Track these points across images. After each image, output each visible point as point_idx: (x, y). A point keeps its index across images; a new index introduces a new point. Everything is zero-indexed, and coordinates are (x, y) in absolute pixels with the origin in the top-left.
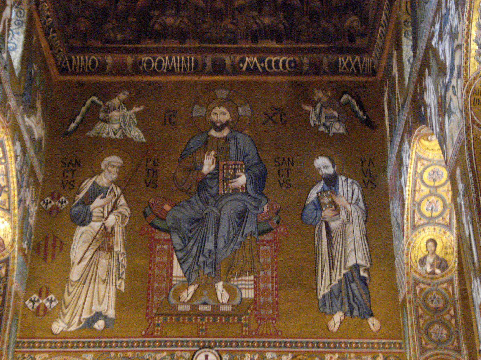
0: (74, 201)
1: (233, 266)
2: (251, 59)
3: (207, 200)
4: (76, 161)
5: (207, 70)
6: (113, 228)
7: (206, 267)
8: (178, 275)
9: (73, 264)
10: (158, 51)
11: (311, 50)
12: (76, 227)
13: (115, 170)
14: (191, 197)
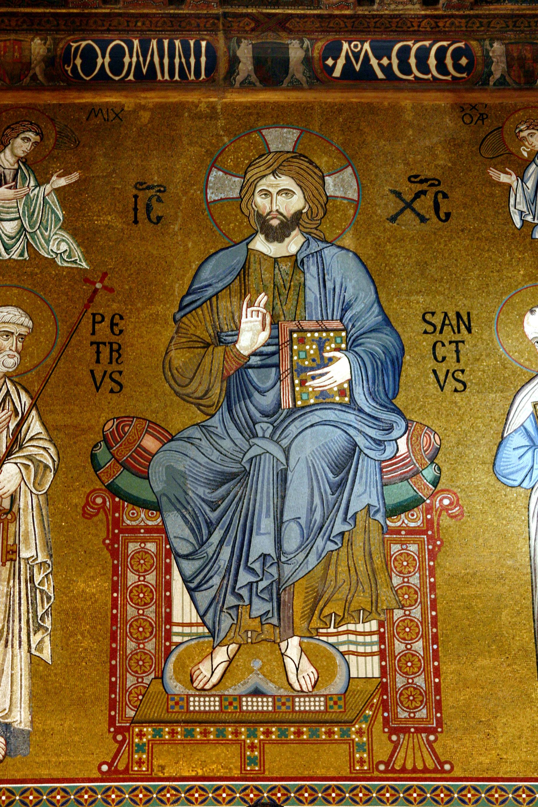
3: (251, 424)
5: (239, 78)
6: (13, 498)
7: (255, 599)
8: (187, 620)
14: (213, 416)
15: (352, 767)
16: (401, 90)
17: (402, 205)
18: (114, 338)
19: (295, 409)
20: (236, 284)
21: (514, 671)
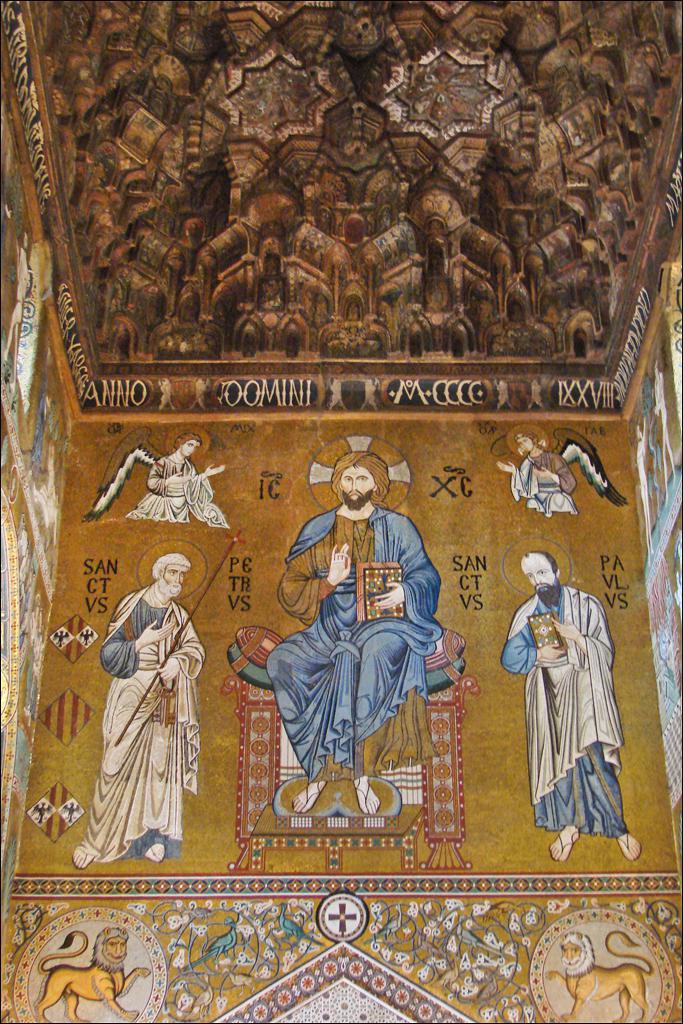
0: (107, 635)
1: (386, 749)
4: (109, 562)
5: (332, 404)
8: (290, 765)
9: (108, 745)
10: (247, 369)
12: (112, 680)
13: (175, 579)
14: (310, 626)
15: (403, 866)
16: (438, 411)
17: (439, 486)
18: (245, 574)
19: (367, 621)
20: (328, 539)
21: (515, 799)
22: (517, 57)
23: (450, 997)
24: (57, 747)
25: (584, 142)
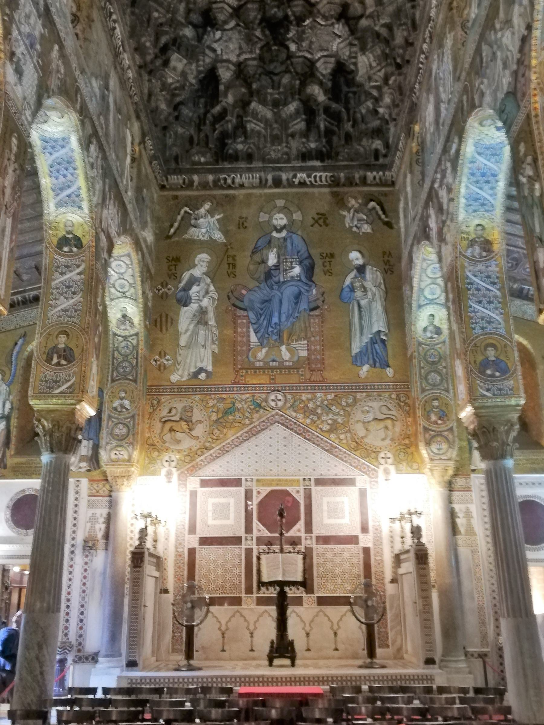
2: (303, 176)
6: (206, 308)
11: (346, 167)
13: (205, 264)
19: (284, 281)
22: (347, 23)
23: (318, 430)
24: (160, 335)
25: (378, 64)
